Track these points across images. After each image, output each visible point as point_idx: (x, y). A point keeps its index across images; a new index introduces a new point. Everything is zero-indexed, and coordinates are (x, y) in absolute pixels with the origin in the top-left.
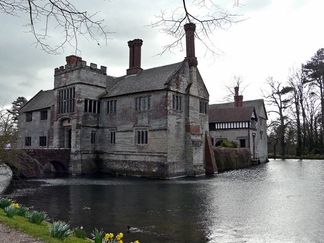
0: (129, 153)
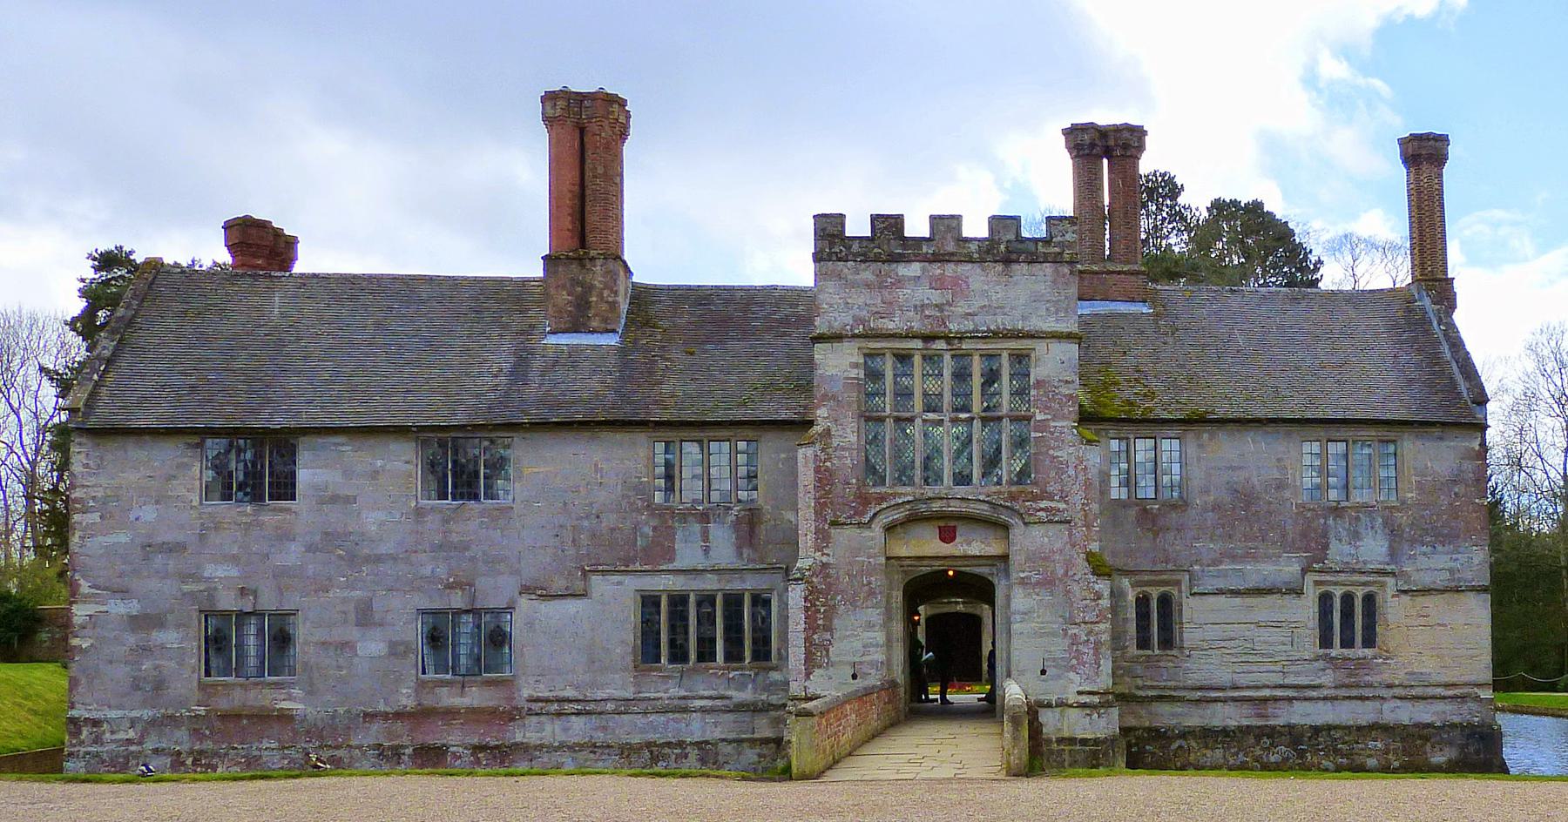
0: (1279, 693)
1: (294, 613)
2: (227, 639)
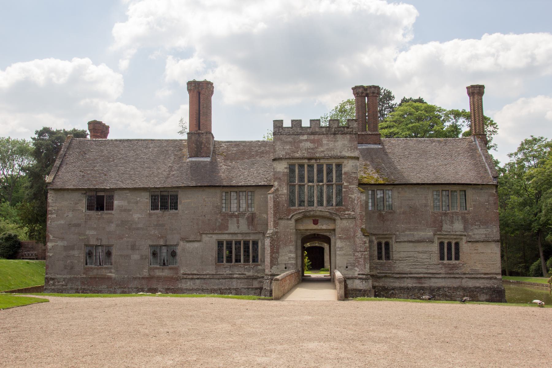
0: (426, 275)
1: (112, 245)
2: (92, 253)
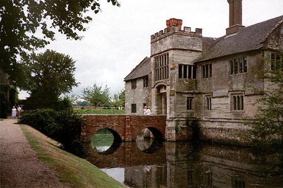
0: (225, 120)
